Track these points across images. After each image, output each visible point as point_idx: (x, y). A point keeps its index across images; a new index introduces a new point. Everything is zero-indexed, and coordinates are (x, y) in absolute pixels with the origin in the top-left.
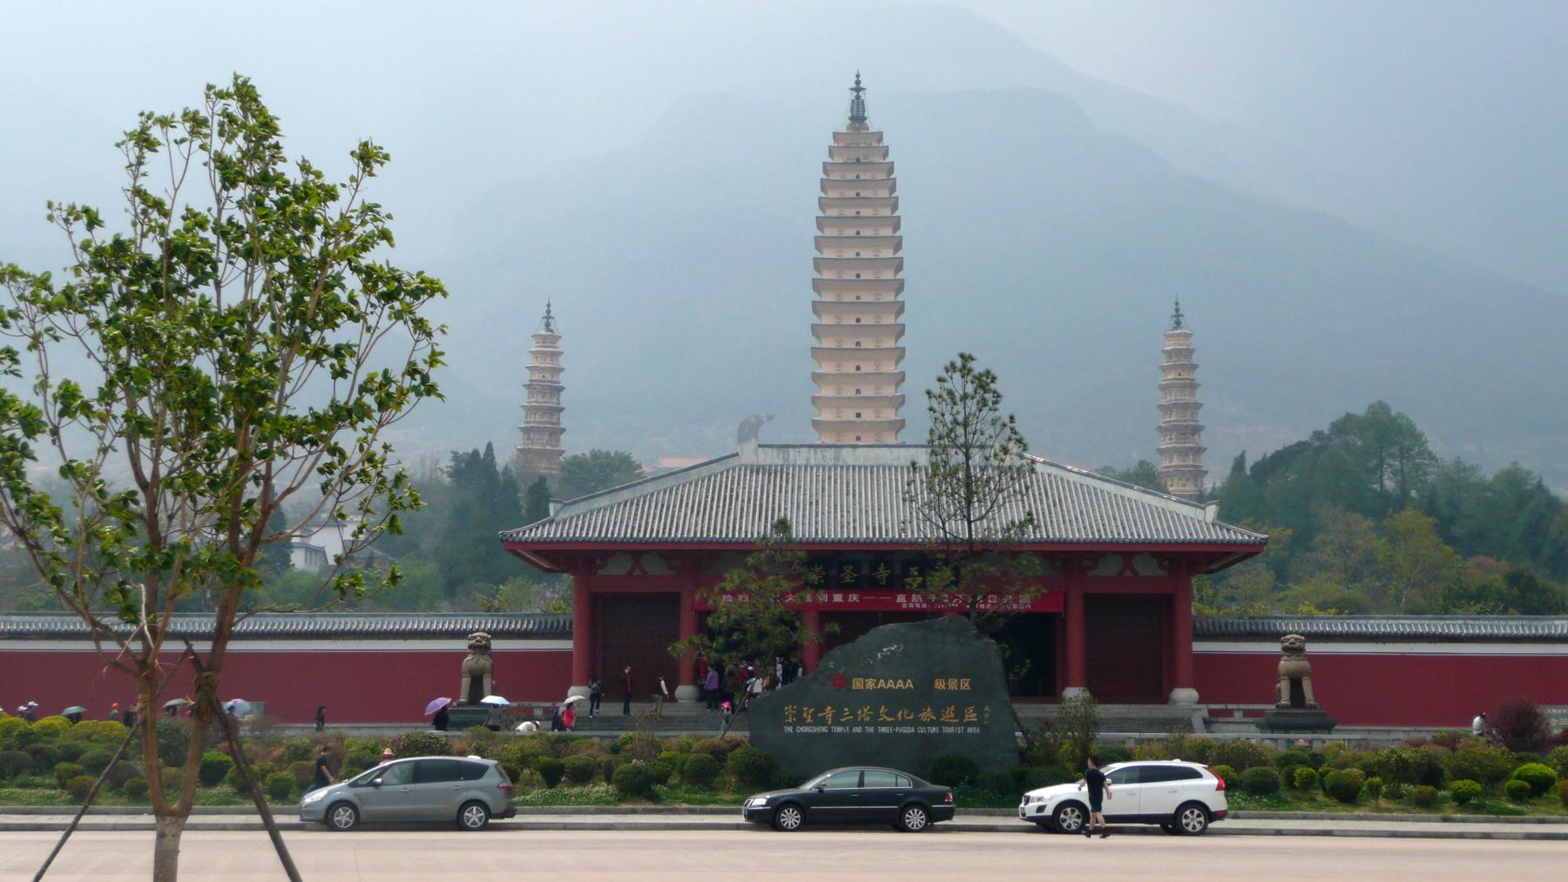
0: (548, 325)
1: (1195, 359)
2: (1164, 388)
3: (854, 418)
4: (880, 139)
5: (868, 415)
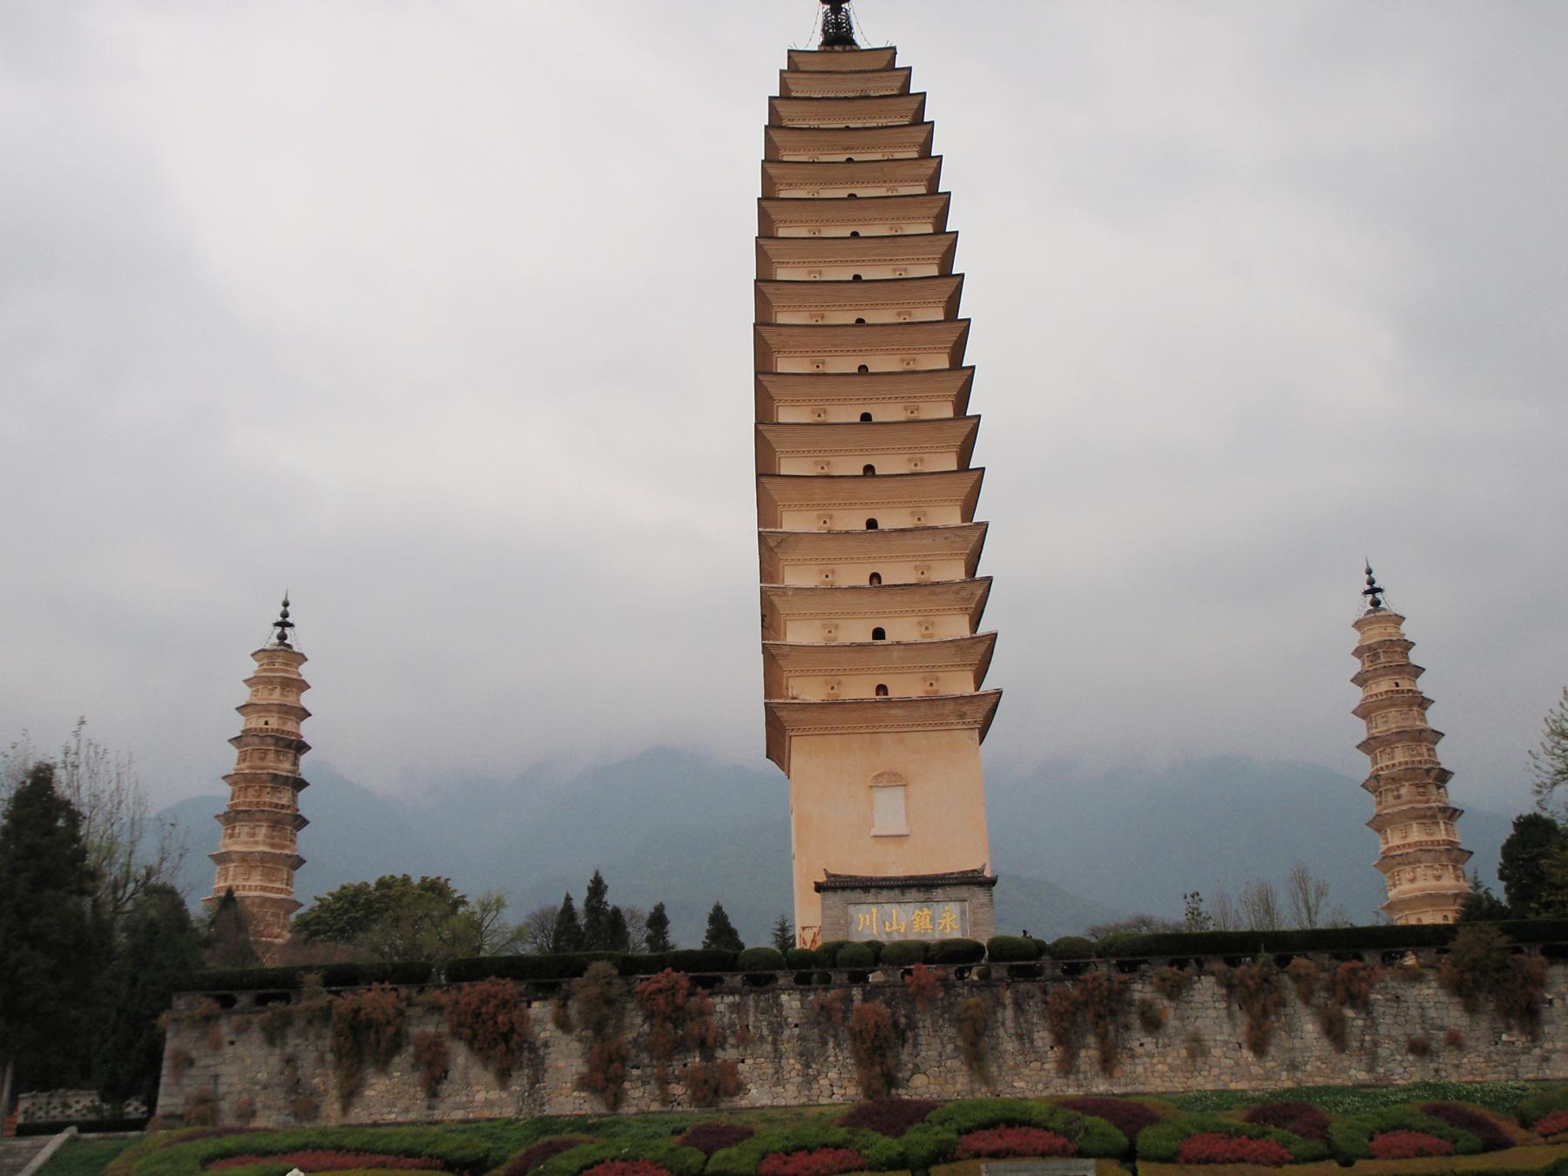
0: (282, 637)
1: (1415, 657)
2: (1364, 712)
3: (869, 639)
4: (891, 66)
5: (901, 630)
